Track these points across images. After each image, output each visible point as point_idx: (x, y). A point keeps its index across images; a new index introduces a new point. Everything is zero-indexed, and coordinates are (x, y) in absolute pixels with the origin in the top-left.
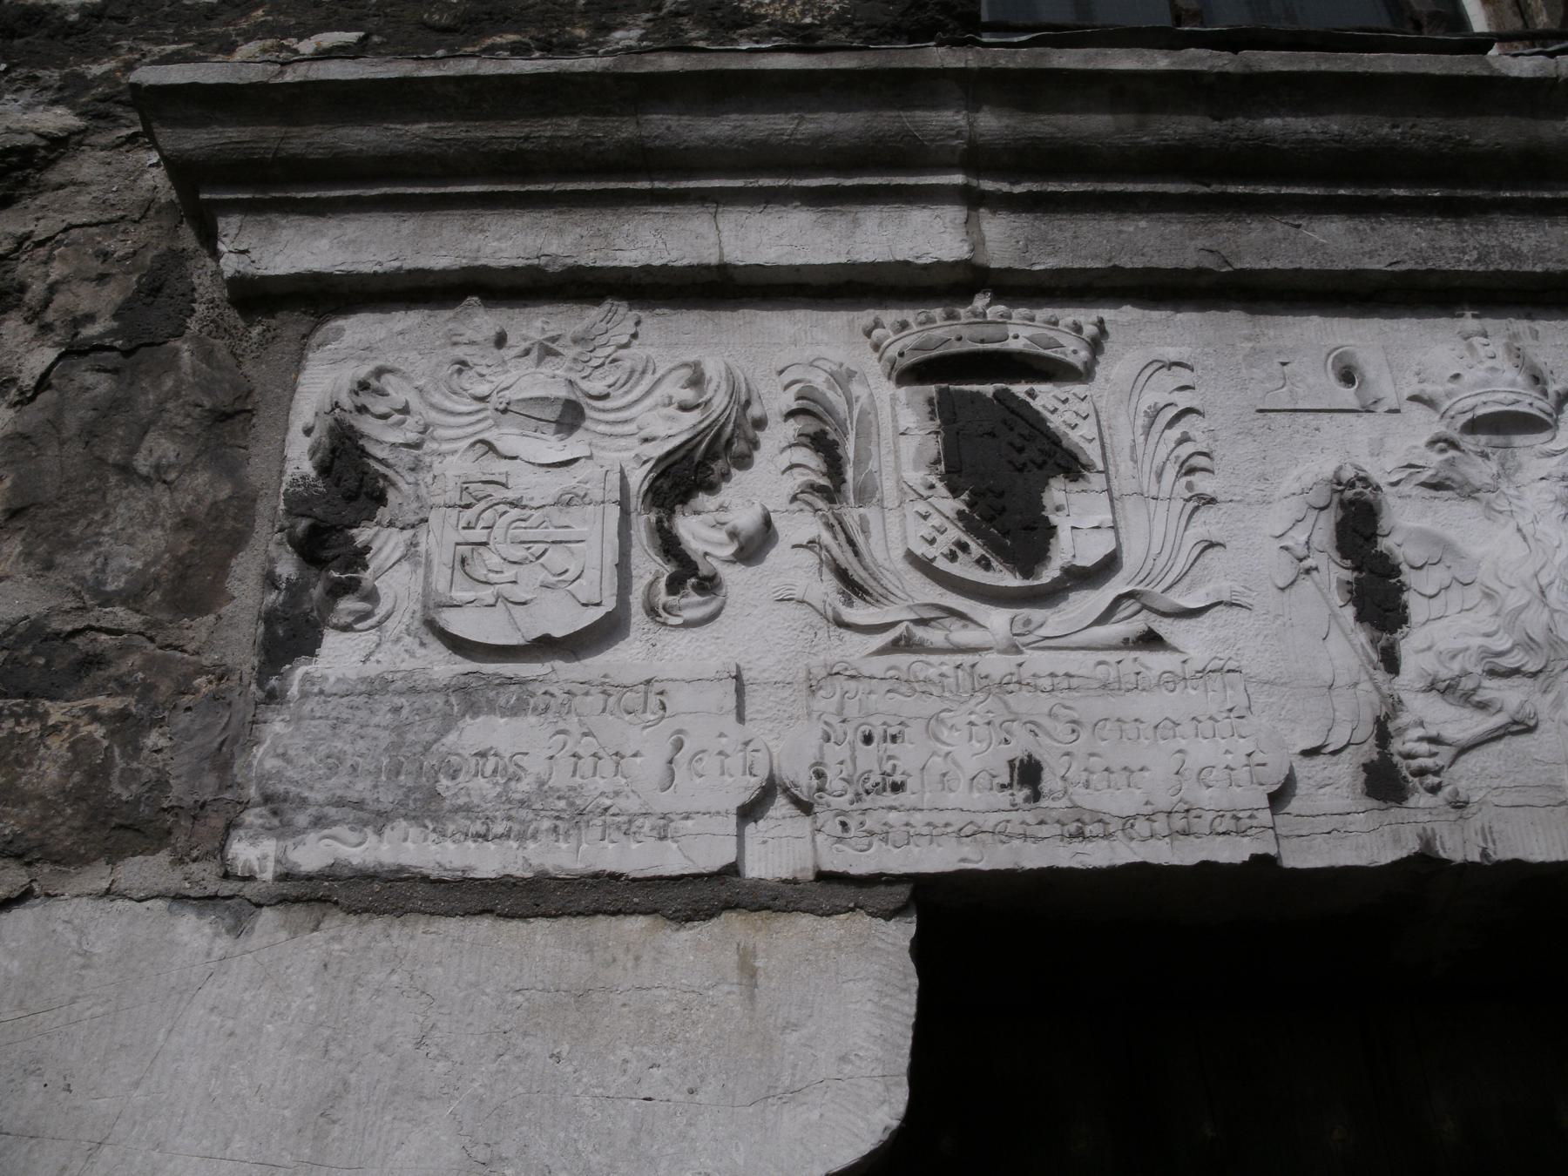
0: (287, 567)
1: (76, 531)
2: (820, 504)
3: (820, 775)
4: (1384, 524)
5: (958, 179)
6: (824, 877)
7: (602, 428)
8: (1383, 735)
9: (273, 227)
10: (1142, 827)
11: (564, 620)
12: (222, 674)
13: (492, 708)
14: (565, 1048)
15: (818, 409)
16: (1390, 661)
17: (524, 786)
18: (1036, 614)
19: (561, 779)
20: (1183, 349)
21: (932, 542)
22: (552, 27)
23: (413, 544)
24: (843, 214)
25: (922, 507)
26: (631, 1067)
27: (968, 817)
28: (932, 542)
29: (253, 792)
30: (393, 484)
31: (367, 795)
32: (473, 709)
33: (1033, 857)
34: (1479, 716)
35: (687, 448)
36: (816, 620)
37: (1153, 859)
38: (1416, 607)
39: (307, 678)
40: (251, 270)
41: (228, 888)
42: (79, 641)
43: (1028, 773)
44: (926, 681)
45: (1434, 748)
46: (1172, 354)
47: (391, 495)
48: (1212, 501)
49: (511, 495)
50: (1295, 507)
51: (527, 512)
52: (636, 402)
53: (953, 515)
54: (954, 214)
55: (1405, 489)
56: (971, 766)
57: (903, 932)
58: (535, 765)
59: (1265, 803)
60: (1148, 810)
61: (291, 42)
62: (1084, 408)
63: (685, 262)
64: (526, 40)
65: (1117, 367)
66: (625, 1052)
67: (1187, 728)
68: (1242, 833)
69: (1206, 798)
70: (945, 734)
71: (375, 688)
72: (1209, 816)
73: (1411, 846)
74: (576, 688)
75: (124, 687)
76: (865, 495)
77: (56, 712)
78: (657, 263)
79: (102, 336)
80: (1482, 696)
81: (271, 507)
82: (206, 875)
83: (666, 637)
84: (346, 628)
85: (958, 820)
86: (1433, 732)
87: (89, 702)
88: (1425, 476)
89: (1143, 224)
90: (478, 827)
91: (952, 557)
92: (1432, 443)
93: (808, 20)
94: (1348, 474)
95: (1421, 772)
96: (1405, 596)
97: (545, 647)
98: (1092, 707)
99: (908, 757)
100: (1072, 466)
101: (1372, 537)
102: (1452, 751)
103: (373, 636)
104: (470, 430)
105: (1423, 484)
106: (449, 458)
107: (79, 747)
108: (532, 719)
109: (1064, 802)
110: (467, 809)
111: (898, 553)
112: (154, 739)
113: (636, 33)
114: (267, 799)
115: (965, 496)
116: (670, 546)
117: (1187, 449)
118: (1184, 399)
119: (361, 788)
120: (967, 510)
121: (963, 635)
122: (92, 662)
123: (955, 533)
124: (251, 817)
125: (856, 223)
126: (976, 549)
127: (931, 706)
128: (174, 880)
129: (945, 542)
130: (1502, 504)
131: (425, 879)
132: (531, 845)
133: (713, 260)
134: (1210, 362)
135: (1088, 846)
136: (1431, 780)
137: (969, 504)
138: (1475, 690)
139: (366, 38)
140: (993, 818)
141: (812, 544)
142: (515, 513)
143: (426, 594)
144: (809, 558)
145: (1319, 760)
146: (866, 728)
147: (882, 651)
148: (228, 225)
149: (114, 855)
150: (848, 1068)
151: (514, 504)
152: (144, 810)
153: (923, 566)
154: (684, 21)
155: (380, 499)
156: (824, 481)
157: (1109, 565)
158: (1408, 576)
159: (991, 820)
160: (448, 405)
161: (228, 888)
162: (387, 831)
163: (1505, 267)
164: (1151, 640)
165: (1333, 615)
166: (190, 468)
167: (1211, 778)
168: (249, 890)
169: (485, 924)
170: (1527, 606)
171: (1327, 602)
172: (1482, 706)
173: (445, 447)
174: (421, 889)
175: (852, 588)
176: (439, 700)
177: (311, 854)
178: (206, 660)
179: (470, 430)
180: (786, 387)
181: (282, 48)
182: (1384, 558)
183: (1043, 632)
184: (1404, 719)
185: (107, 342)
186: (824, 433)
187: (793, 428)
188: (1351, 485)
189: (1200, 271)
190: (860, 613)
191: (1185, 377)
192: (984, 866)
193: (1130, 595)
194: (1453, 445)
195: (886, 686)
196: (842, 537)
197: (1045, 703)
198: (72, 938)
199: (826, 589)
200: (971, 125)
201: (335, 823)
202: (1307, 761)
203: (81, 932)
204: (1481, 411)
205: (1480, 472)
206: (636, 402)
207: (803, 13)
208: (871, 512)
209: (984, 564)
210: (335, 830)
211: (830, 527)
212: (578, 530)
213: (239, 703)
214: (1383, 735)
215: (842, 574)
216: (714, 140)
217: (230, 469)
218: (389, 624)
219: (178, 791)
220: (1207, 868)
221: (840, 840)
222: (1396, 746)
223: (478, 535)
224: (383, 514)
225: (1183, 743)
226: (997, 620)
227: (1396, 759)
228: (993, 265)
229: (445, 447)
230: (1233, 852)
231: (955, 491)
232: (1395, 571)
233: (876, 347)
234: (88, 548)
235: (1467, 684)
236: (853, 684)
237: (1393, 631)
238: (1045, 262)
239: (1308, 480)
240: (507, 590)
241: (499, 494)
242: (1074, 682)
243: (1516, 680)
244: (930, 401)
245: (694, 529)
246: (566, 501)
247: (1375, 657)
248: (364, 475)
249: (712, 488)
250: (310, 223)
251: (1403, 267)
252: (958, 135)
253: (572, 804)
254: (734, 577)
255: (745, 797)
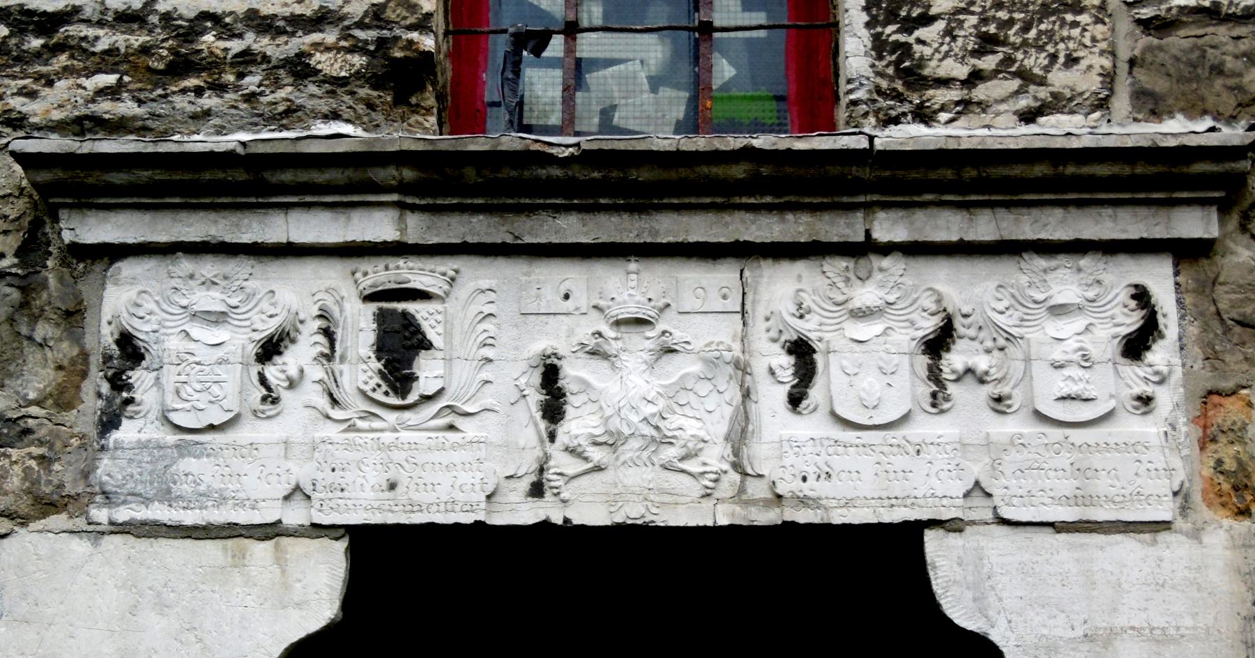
0: (105, 388)
1: (12, 368)
2: (325, 362)
3: (314, 484)
4: (561, 375)
5: (395, 197)
6: (314, 525)
7: (236, 323)
8: (541, 470)
9: (85, 216)
10: (435, 508)
11: (218, 418)
12: (83, 436)
13: (190, 454)
14: (217, 588)
15: (327, 315)
16: (552, 437)
17: (202, 488)
18: (407, 415)
19: (217, 485)
20: (492, 281)
21: (366, 383)
22: (215, 74)
23: (158, 379)
24: (344, 213)
25: (365, 367)
26: (240, 596)
27: (369, 502)
28: (366, 383)
29: (97, 489)
30: (147, 350)
31: (142, 491)
32: (182, 456)
33: (391, 519)
34: (583, 463)
35: (270, 338)
36: (322, 417)
37: (437, 521)
38: (570, 411)
39: (116, 441)
40: (76, 240)
41: (91, 528)
42: (21, 423)
43: (392, 486)
44: (360, 445)
45: (559, 477)
46: (485, 284)
47: (147, 356)
48: (491, 361)
49: (197, 359)
50: (523, 366)
51: (203, 367)
52: (250, 310)
53: (376, 371)
54: (392, 214)
55: (579, 354)
56: (372, 481)
57: (341, 546)
58: (207, 479)
59: (484, 499)
60: (438, 501)
61: (83, 81)
62: (440, 318)
63: (271, 241)
64: (202, 84)
65: (463, 290)
66: (238, 590)
67: (460, 467)
68: (473, 511)
69: (460, 497)
70: (363, 468)
71: (143, 446)
72: (460, 504)
73: (543, 518)
74: (223, 446)
75: (41, 443)
76: (343, 359)
77: (15, 453)
78: (260, 241)
79: (10, 267)
80: (586, 454)
81: (95, 360)
82: (81, 523)
83: (259, 422)
84: (131, 418)
85: (364, 503)
86: (559, 471)
87: (27, 450)
88: (587, 349)
89: (481, 217)
90: (185, 505)
91: (374, 390)
92: (593, 334)
93: (343, 74)
94: (549, 352)
95: (551, 488)
96: (565, 407)
97: (212, 428)
98: (421, 458)
99: (350, 476)
100: (428, 346)
101: (556, 381)
102: (567, 479)
103: (142, 421)
104: (180, 322)
105: (587, 352)
106: (171, 337)
107: (27, 471)
108: (205, 459)
109: (406, 497)
110: (180, 497)
111: (354, 386)
112: (57, 467)
113: (256, 79)
114: (104, 493)
115: (383, 362)
116: (263, 380)
117: (486, 335)
118: (488, 309)
119: (140, 489)
120: (382, 367)
121: (376, 424)
122: (27, 431)
123: (377, 380)
124: (98, 498)
125: (349, 218)
126: (384, 388)
127: (359, 456)
128: (69, 525)
129: (372, 383)
130: (618, 364)
131: (165, 525)
132: (204, 511)
133: (285, 241)
134: (505, 288)
135: (412, 515)
136: (555, 491)
137: (385, 366)
138: (583, 452)
139: (121, 78)
140: (378, 503)
141: (320, 381)
142: (198, 367)
143: (163, 404)
144: (318, 387)
145: (512, 481)
146: (333, 465)
147: (345, 431)
148: (63, 214)
149: (44, 515)
150: (317, 596)
151: (198, 363)
152: (55, 497)
153: (363, 393)
154: (282, 71)
155: (142, 357)
156: (327, 351)
157: (440, 392)
158: (570, 398)
159: (376, 504)
160: (170, 310)
161: (91, 528)
162: (150, 505)
163: (649, 240)
164: (451, 427)
165: (531, 416)
166: (60, 340)
167: (464, 488)
168: (99, 528)
169: (188, 541)
170: (612, 416)
171: (530, 410)
172: (586, 459)
173: (170, 331)
174: (164, 529)
175: (334, 402)
176: (170, 450)
177: (123, 514)
178: (76, 430)
179: (180, 322)
180: (315, 303)
181: (80, 86)
182: (560, 389)
183: (409, 423)
184: (552, 463)
185: (14, 270)
186: (329, 327)
187: (319, 323)
188: (549, 357)
189: (504, 244)
190: (337, 414)
191: (492, 296)
192: (372, 522)
193: (448, 407)
194: (600, 334)
195: (344, 447)
196: (332, 378)
197: (404, 455)
198: (31, 548)
199: (323, 402)
200: (400, 174)
201: (131, 502)
202: (508, 481)
203: (35, 546)
204: (620, 317)
205: (613, 347)
206: (250, 310)
207: (341, 68)
208: (345, 367)
209: (386, 394)
210: (131, 506)
211: (327, 373)
212: (224, 376)
213: (90, 449)
214: (541, 470)
215: (331, 395)
216: (283, 182)
217: (77, 340)
218: (149, 415)
219: (69, 489)
220: (457, 525)
221: (320, 511)
222: (546, 475)
223: (183, 378)
224: (144, 363)
225: (455, 473)
226: (392, 417)
227: (544, 481)
228: (410, 242)
229: (170, 331)
230: (467, 519)
231: (379, 359)
232: (564, 395)
233: (356, 282)
234: (18, 378)
235: (580, 450)
236: (330, 446)
237: (556, 424)
238: (435, 240)
239: (532, 354)
240: (195, 403)
241: (192, 359)
242: (418, 446)
243: (604, 447)
244: (374, 315)
245: (271, 372)
246: (222, 362)
247: (545, 435)
248: (136, 348)
249: (280, 353)
250: (102, 214)
251: (600, 241)
252: (394, 178)
253: (221, 495)
254: (286, 396)
255: (286, 493)
